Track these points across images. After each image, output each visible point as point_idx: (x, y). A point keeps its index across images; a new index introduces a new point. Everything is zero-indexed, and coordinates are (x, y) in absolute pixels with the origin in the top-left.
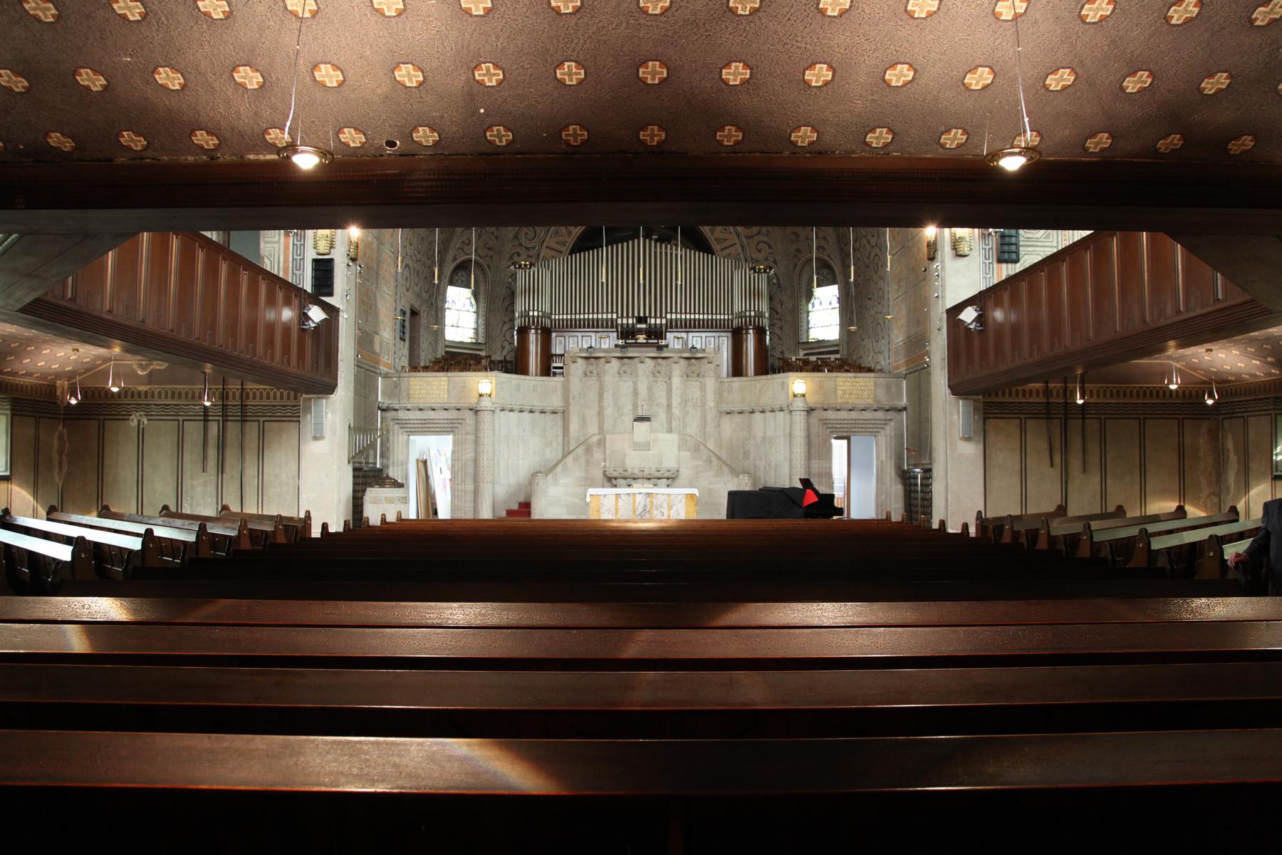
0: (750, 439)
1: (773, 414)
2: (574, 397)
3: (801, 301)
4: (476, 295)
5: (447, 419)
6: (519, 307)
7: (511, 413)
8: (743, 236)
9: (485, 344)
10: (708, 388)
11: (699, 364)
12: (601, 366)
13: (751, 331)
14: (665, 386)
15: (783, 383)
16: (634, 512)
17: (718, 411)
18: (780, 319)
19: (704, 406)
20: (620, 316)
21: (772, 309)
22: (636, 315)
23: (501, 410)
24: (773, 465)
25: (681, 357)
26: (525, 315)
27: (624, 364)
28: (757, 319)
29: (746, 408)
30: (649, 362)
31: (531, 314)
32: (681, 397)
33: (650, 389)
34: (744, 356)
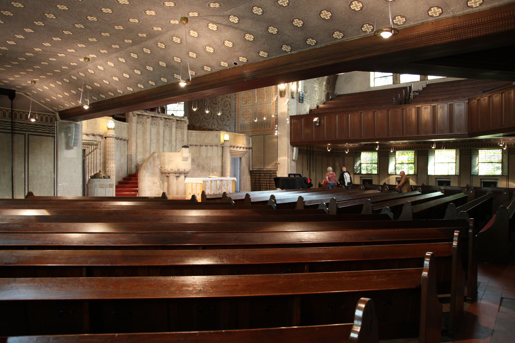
0: (200, 157)
1: (211, 147)
2: (134, 133)
5: (87, 140)
10: (185, 133)
15: (217, 135)
16: (217, 188)
24: (211, 167)
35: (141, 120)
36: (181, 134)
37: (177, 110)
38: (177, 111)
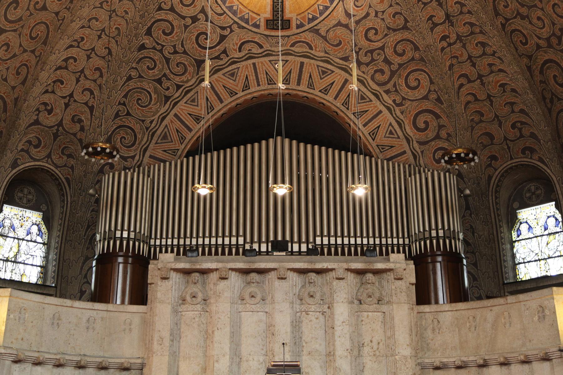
3: (500, 227)
4: (47, 220)
6: (103, 226)
7: (39, 368)
8: (415, 142)
9: (56, 287)
11: (380, 283)
12: (211, 286)
13: (440, 259)
14: (322, 318)
15: (542, 308)
17: (419, 364)
18: (473, 252)
19: (392, 355)
20: (248, 240)
21: (469, 229)
22: (272, 238)
23: (16, 362)
25: (348, 270)
26: (110, 236)
27: (249, 283)
28: (447, 241)
29: (471, 358)
30: (293, 277)
31: (118, 234)
32: (351, 339)
33: (296, 325)
34: (432, 295)
35: (195, 289)
36: (384, 323)
37: (546, 257)
38: (548, 260)
